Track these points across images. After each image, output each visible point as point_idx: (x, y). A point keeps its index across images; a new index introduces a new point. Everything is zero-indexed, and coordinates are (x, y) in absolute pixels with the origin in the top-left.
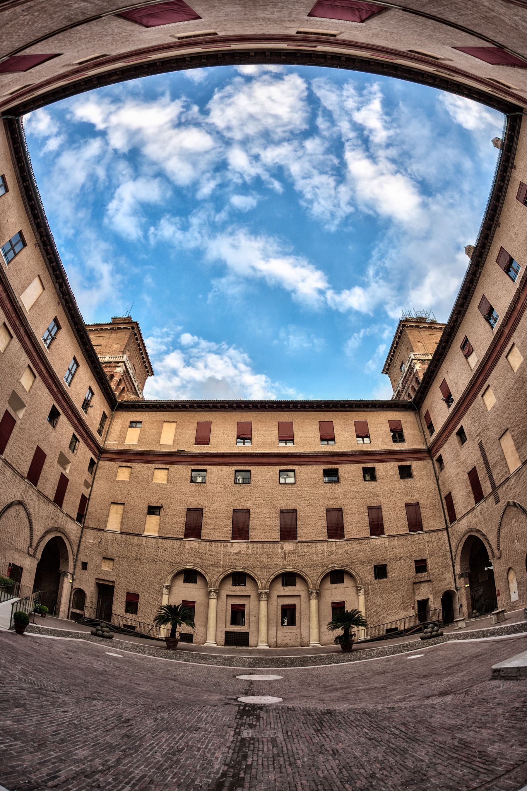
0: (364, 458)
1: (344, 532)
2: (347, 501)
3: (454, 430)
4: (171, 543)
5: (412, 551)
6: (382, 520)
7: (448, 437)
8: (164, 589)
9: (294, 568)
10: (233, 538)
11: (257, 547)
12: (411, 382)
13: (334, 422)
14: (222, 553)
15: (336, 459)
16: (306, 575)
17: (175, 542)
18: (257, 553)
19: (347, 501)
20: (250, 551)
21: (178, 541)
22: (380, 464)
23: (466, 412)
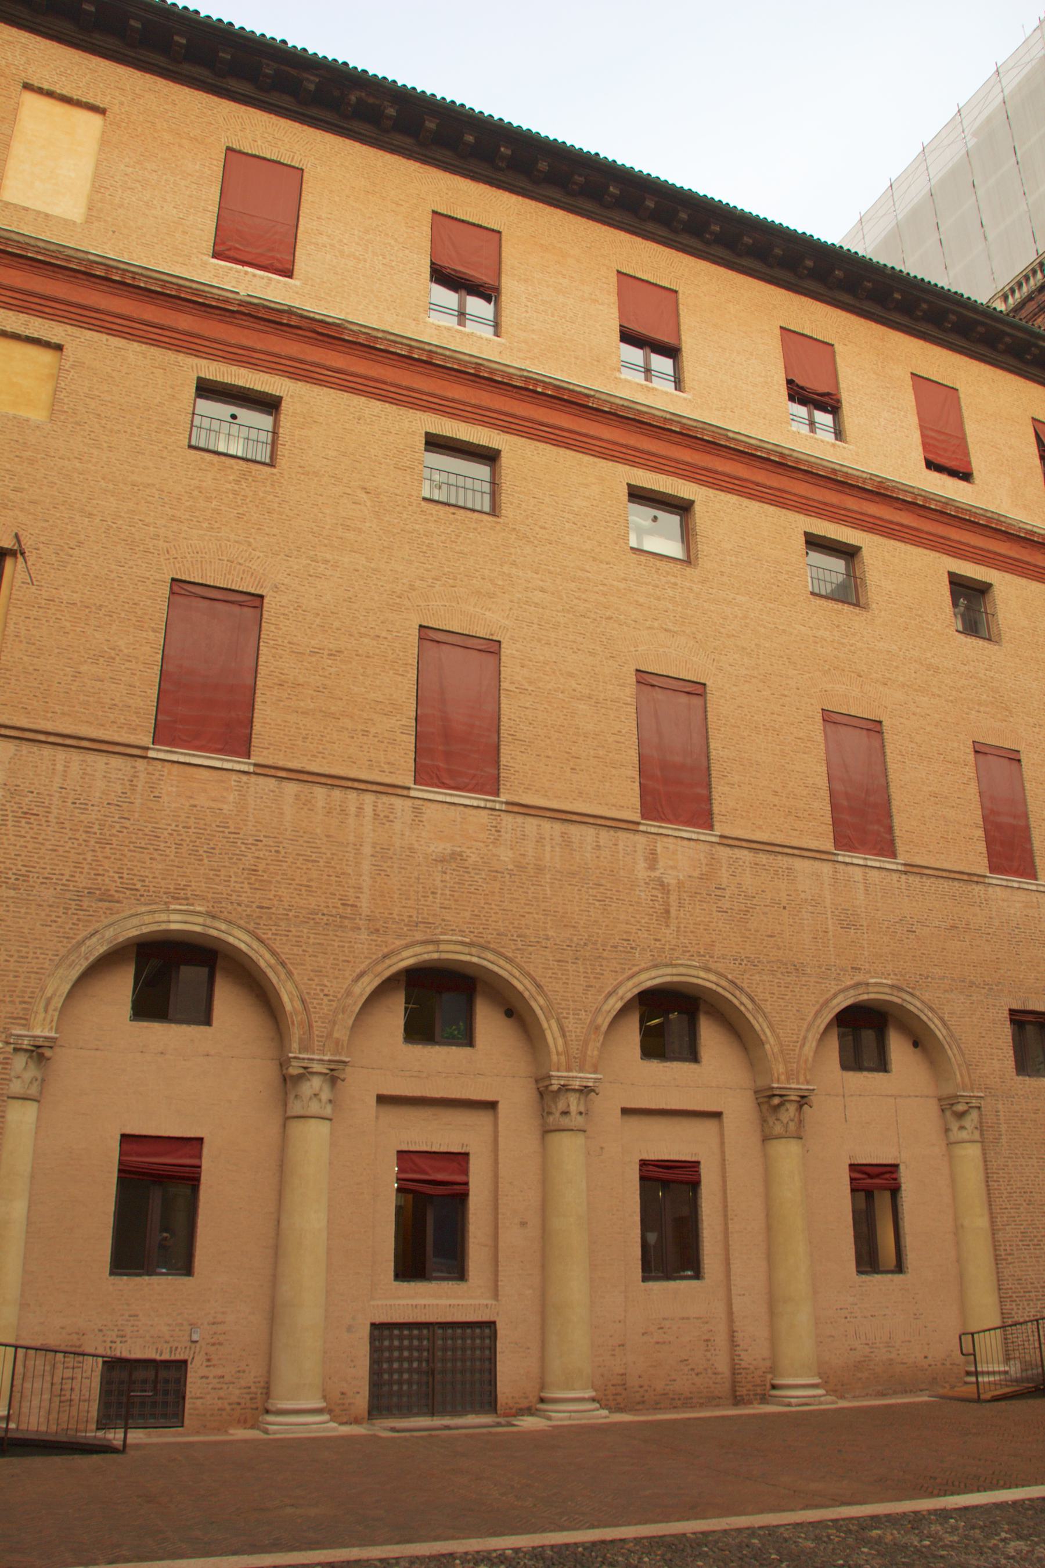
0: (955, 534)
1: (890, 829)
4: (75, 768)
6: (1026, 816)
8: (20, 1062)
9: (708, 970)
10: (424, 774)
11: (540, 840)
13: (838, 348)
14: (367, 850)
15: (851, 503)
16: (758, 1008)
17: (99, 763)
18: (540, 869)
20: (506, 856)
21: (116, 762)
22: (1008, 577)
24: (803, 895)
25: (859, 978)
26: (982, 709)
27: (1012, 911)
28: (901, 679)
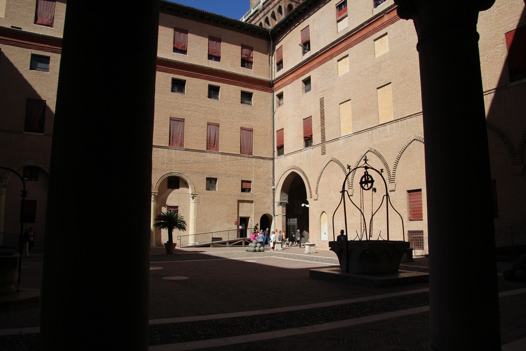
2: (190, 113)
3: (301, 76)
5: (240, 172)
7: (294, 80)
12: (273, 7)
19: (190, 113)
23: (318, 66)
24: (160, 155)
25: (171, 171)
26: (211, 115)
27: (211, 158)
28: (191, 109)
